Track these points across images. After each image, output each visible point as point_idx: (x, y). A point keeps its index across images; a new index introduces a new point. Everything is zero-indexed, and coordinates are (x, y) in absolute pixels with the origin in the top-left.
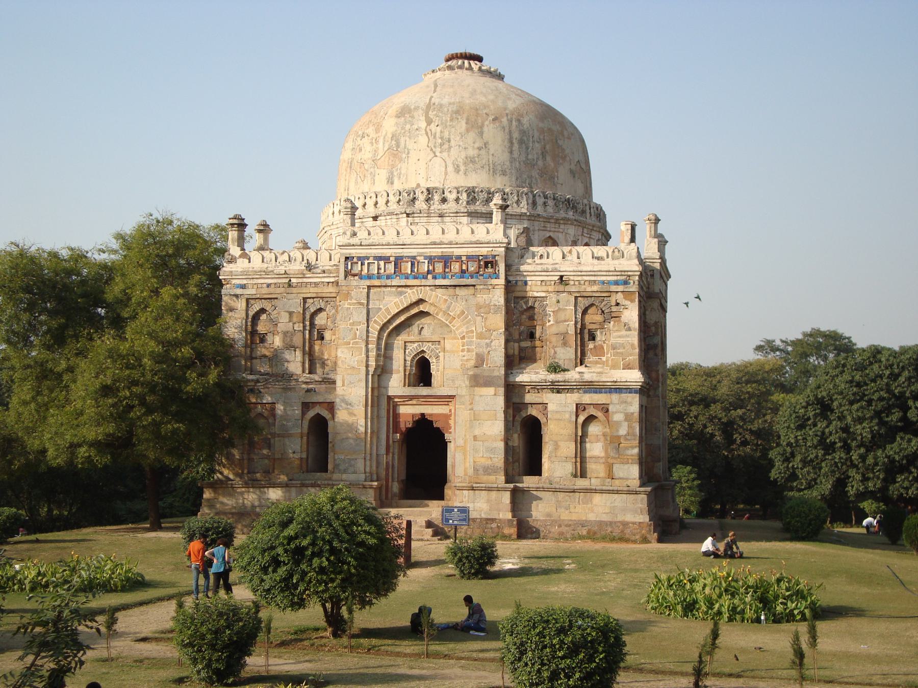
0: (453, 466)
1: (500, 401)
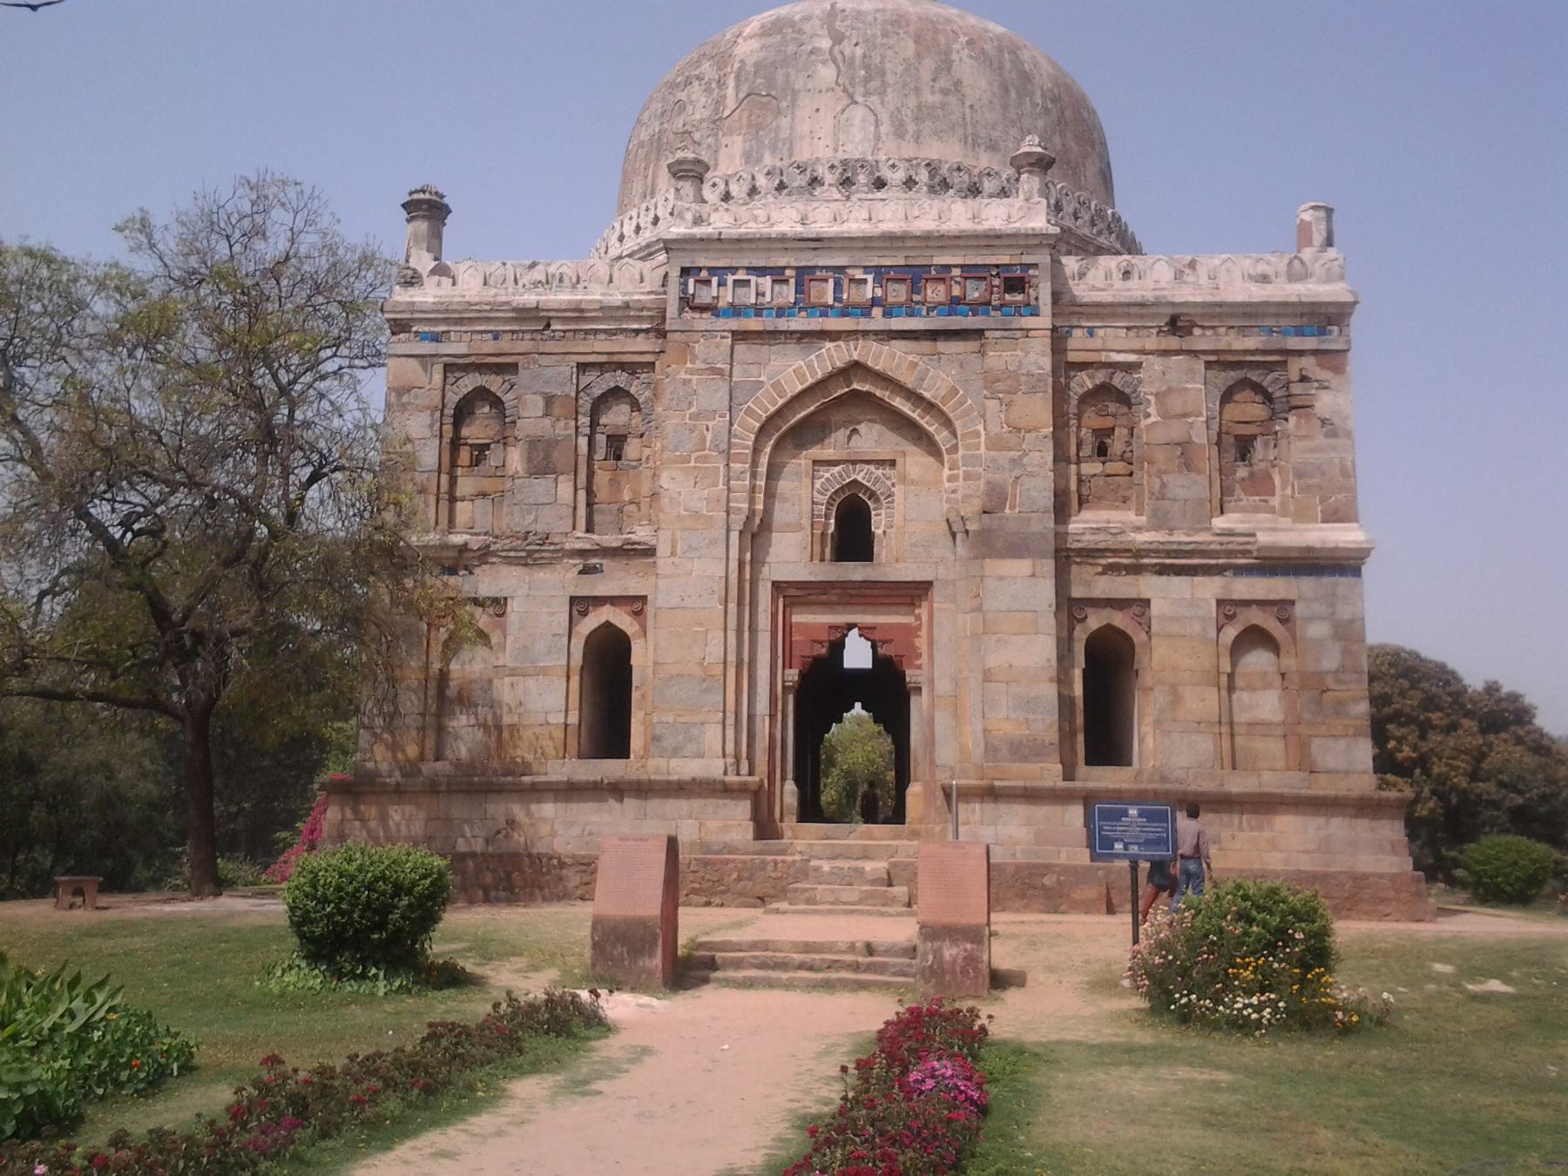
0: (931, 743)
1: (1046, 591)
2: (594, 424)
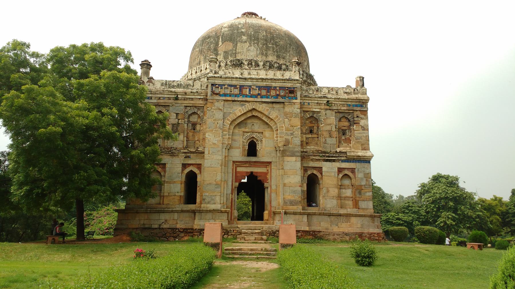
1: (299, 164)
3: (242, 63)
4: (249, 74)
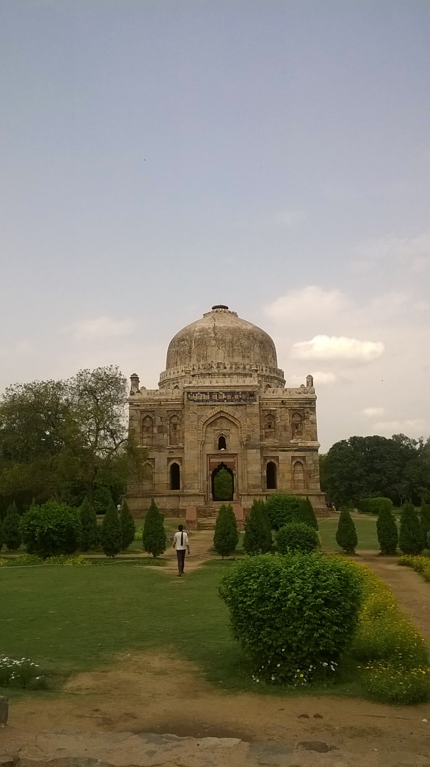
1: (259, 455)
2: (170, 422)
3: (212, 367)
4: (217, 382)
